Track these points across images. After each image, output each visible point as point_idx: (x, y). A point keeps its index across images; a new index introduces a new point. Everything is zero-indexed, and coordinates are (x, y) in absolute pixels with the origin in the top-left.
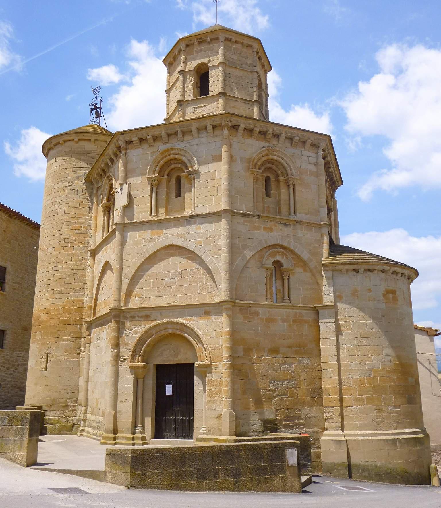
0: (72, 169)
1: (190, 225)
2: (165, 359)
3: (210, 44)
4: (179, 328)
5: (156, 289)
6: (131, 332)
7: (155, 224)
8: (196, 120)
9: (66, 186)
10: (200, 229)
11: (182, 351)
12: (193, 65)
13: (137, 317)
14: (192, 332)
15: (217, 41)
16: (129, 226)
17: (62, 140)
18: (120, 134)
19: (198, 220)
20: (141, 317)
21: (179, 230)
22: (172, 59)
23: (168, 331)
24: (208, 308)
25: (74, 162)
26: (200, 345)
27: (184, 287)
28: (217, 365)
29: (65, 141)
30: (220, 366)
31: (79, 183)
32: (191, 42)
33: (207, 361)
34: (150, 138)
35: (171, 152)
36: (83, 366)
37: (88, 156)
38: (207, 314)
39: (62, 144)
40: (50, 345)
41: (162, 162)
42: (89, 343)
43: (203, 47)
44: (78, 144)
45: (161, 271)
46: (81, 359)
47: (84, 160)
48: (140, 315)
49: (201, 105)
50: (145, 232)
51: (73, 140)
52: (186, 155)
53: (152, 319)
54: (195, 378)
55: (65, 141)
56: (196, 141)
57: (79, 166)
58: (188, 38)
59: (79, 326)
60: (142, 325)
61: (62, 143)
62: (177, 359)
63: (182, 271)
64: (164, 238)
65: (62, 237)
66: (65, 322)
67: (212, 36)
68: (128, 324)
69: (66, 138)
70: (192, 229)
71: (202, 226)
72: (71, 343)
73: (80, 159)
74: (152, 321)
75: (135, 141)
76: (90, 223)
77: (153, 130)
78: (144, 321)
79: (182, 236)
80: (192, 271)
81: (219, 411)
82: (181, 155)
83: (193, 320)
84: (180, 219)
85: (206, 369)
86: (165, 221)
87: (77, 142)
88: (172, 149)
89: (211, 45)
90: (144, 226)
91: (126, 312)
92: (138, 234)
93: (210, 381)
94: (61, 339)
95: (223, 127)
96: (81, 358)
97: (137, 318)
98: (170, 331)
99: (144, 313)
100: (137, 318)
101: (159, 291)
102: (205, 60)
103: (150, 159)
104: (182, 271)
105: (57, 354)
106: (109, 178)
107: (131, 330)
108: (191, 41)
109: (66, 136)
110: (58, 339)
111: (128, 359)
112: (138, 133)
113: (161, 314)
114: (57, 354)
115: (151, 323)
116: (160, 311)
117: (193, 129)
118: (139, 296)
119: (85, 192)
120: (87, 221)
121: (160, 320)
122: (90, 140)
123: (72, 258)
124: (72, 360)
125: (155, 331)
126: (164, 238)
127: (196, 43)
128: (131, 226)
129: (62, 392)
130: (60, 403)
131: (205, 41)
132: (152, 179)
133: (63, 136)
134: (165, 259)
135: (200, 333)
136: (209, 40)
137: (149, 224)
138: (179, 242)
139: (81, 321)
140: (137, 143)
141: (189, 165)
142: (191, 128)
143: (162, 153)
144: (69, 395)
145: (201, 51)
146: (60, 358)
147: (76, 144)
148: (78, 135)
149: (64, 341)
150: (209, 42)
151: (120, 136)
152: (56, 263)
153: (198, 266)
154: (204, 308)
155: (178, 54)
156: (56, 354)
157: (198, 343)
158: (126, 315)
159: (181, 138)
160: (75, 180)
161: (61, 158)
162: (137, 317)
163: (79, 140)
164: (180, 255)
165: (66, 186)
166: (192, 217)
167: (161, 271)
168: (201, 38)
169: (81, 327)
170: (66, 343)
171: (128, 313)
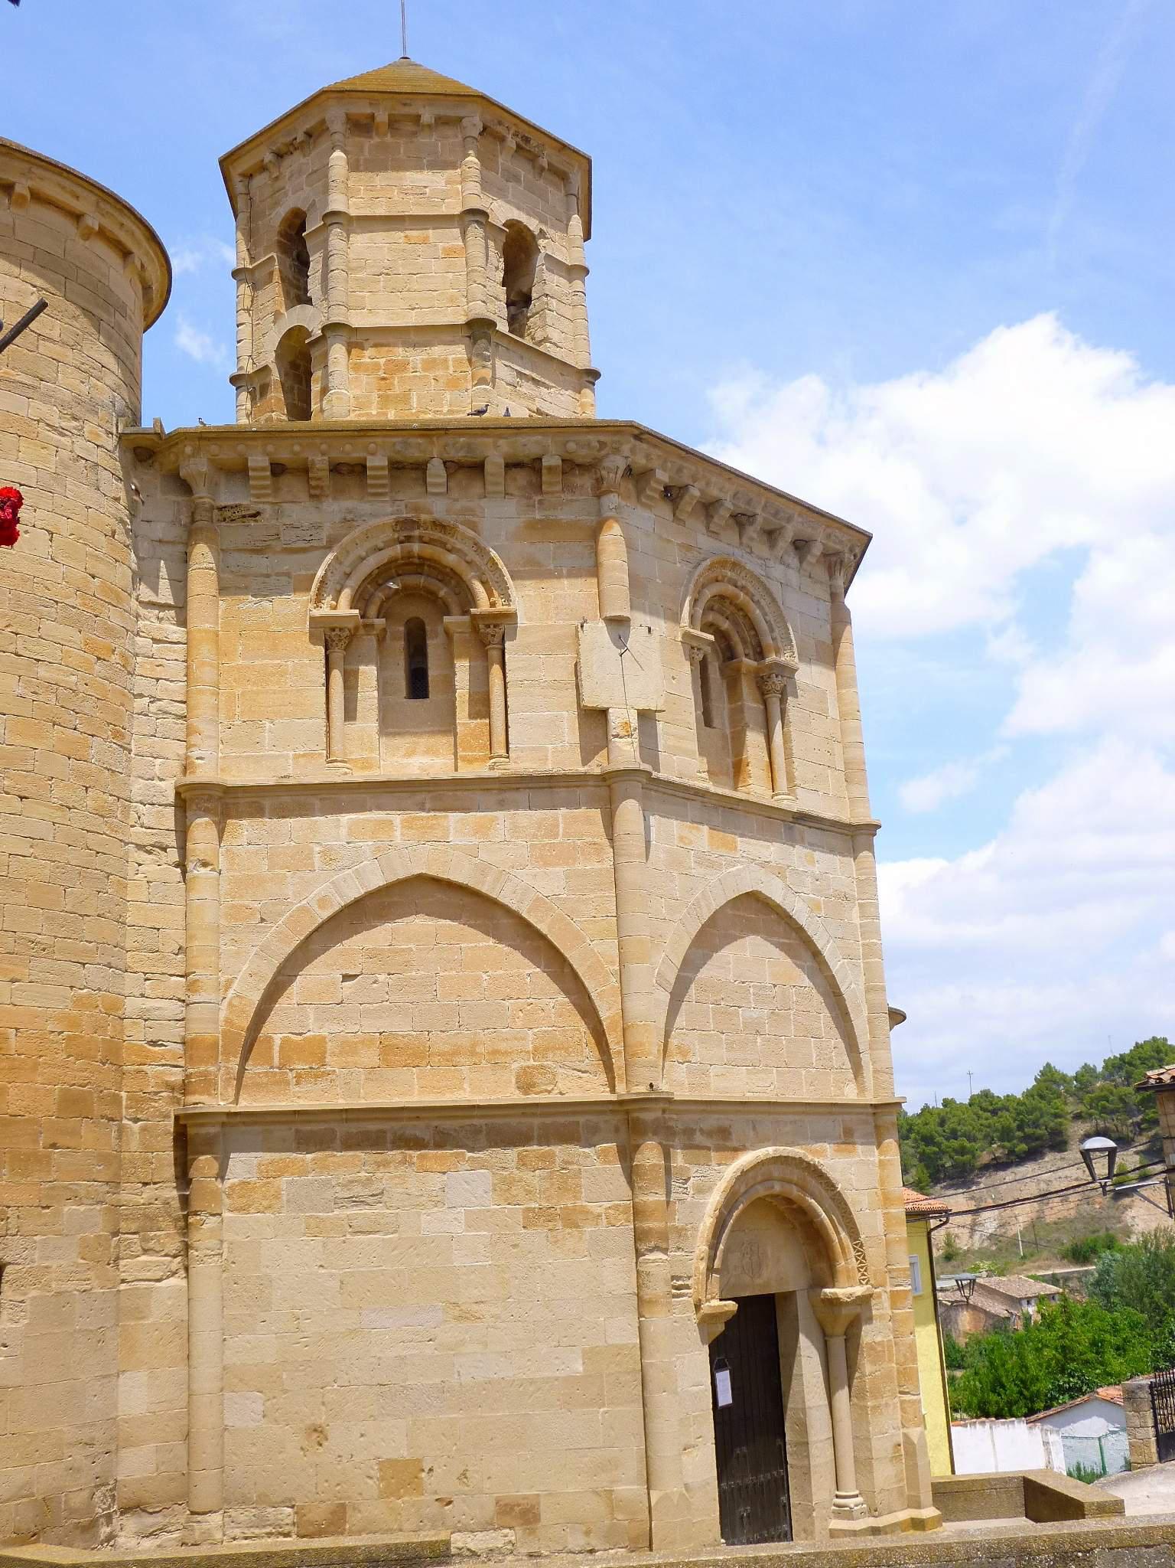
0: (69, 352)
1: (791, 841)
2: (733, 1280)
3: (540, 175)
4: (795, 1179)
5: (723, 1036)
6: (687, 1188)
7: (716, 807)
8: (809, 513)
9: (48, 425)
10: (812, 862)
11: (769, 1253)
12: (502, 212)
13: (698, 1133)
14: (824, 1192)
15: (556, 180)
16: (651, 790)
17: (30, 183)
18: (637, 432)
19: (810, 834)
20: (709, 1134)
21: (771, 851)
22: (382, 117)
23: (773, 1187)
24: (846, 1117)
25: (77, 325)
26: (843, 1235)
27: (784, 1042)
28: (879, 1296)
29: (37, 197)
30: (885, 1297)
31: (98, 435)
32: (500, 129)
33: (867, 1283)
34: (693, 497)
35: (729, 574)
36: (143, 1318)
37: (119, 325)
38: (847, 1138)
39: (21, 202)
40: (13, 1221)
41: (708, 593)
42: (220, 1215)
43: (523, 170)
44: (87, 243)
45: (731, 978)
46: (123, 1287)
47: (109, 338)
48: (705, 1126)
49: (538, 378)
50: (693, 828)
51: (77, 217)
52: (763, 603)
53: (735, 1144)
54: (804, 1342)
55: (37, 197)
56: (777, 571)
57: (96, 356)
58: (499, 110)
59: (114, 1125)
60: (713, 1163)
61: (22, 196)
62: (759, 1281)
63: (775, 986)
64: (740, 867)
65: (42, 671)
66: (74, 1104)
67: (558, 160)
68: (679, 1158)
69: (50, 187)
70: (797, 855)
71: (817, 855)
72: (98, 1207)
73: (97, 322)
74: (736, 1150)
75: (658, 482)
76: (134, 643)
77: (714, 479)
78: (718, 1149)
79: (780, 873)
80: (798, 994)
81: (893, 1435)
82: (752, 597)
83: (821, 1153)
84: (773, 816)
85: (858, 1310)
86: (740, 808)
87: (88, 234)
88: (735, 565)
89: (542, 181)
90: (689, 803)
91: (677, 1113)
92: (675, 825)
93: (872, 1347)
94: (66, 1188)
95: (838, 567)
96: (123, 1281)
97: (699, 1139)
98: (777, 1188)
99: (712, 1121)
100: (699, 1139)
101: (730, 1047)
102: (533, 225)
103: (678, 565)
104: (775, 986)
105: (54, 1264)
106: (413, 529)
107: (687, 1180)
108: (500, 123)
109: (59, 179)
110: (52, 1188)
111: (687, 1287)
112: (680, 462)
113: (754, 1128)
114: (54, 1264)
115: (733, 1159)
116: (752, 1117)
117: (789, 534)
118: (684, 1052)
119: (118, 489)
120: (127, 631)
121: (754, 1148)
122: (126, 254)
123: (87, 788)
124: (103, 1293)
125: (744, 1185)
126: (740, 867)
127: (511, 143)
128: (656, 791)
129: (78, 1456)
130: (72, 1512)
131: (532, 159)
132: (695, 644)
133: (48, 175)
134: (735, 939)
135: (849, 1197)
136: (544, 162)
137: (702, 802)
138: (775, 891)
139: (117, 1100)
140: (655, 490)
141: (767, 640)
142: (782, 528)
143: (711, 568)
144: (97, 1469)
145: (516, 179)
146: (64, 1287)
147: (82, 242)
148: (108, 208)
149: (75, 1198)
150: (542, 169)
151: (632, 440)
152: (22, 798)
153: (807, 982)
154: (840, 1118)
155: (429, 126)
156: (47, 1267)
157: (840, 1229)
158: (670, 1124)
159: (752, 539)
160: (88, 416)
161: (16, 270)
162: (698, 1133)
163: (102, 234)
164: (769, 935)
165: (48, 425)
166: (802, 818)
167: (731, 978)
168: (527, 140)
169: (121, 1130)
170: (82, 1208)
171: (675, 1116)
